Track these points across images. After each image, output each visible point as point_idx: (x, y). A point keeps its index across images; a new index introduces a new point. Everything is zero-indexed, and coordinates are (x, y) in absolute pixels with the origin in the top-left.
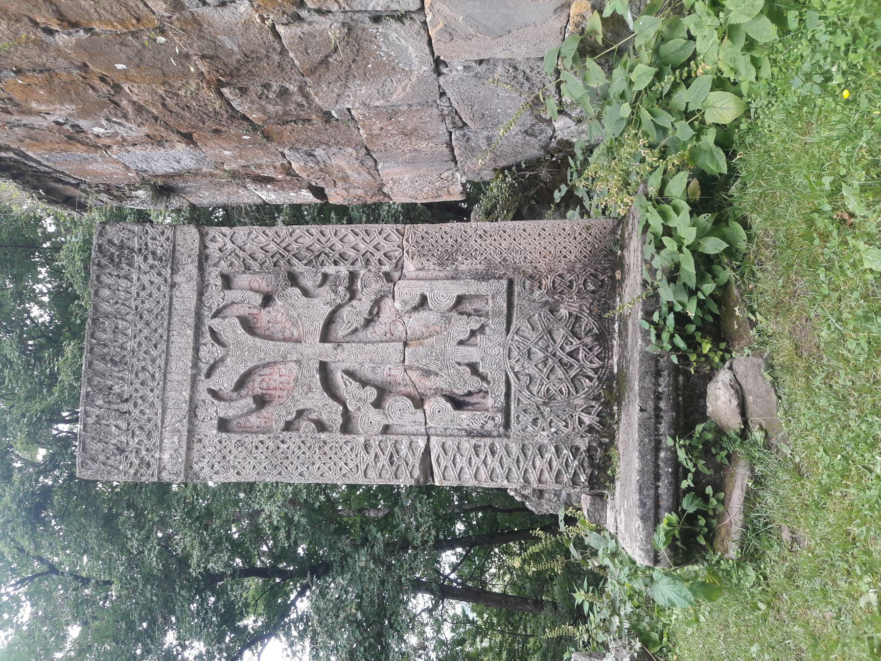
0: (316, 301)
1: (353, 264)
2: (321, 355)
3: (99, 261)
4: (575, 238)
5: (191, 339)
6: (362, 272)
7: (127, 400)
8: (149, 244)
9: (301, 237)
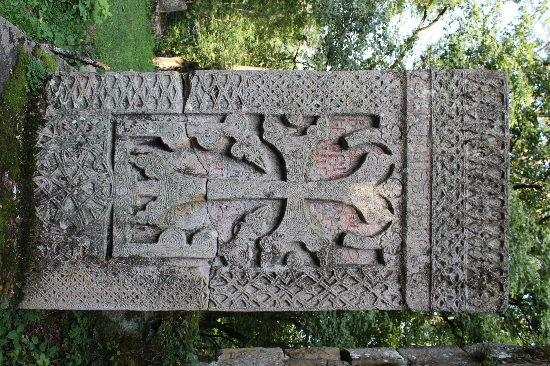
0: (291, 238)
1: (258, 274)
2: (285, 188)
3: (501, 274)
4: (54, 292)
5: (410, 201)
6: (249, 265)
7: (466, 142)
8: (454, 292)
9: (309, 300)
